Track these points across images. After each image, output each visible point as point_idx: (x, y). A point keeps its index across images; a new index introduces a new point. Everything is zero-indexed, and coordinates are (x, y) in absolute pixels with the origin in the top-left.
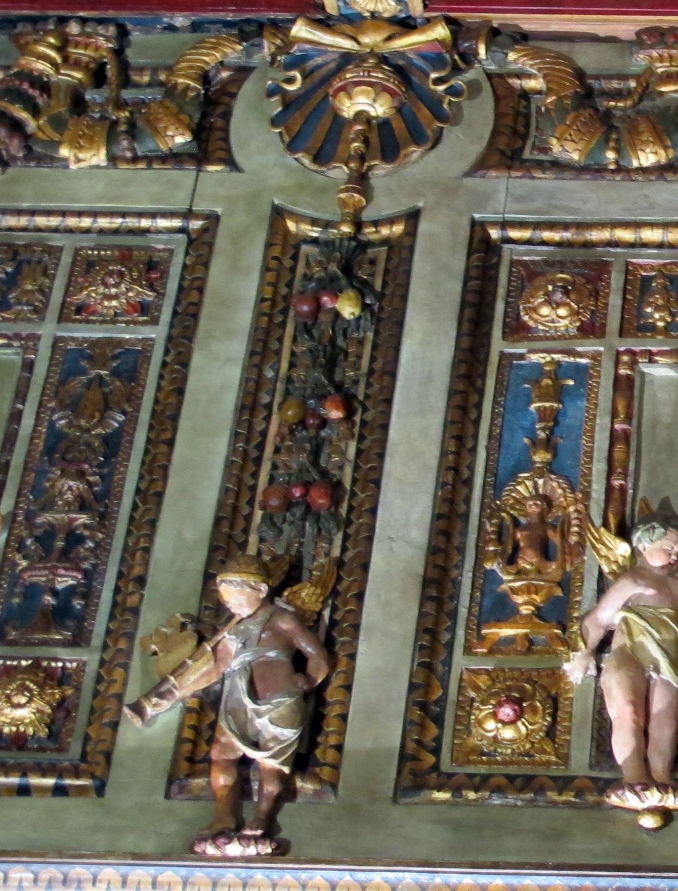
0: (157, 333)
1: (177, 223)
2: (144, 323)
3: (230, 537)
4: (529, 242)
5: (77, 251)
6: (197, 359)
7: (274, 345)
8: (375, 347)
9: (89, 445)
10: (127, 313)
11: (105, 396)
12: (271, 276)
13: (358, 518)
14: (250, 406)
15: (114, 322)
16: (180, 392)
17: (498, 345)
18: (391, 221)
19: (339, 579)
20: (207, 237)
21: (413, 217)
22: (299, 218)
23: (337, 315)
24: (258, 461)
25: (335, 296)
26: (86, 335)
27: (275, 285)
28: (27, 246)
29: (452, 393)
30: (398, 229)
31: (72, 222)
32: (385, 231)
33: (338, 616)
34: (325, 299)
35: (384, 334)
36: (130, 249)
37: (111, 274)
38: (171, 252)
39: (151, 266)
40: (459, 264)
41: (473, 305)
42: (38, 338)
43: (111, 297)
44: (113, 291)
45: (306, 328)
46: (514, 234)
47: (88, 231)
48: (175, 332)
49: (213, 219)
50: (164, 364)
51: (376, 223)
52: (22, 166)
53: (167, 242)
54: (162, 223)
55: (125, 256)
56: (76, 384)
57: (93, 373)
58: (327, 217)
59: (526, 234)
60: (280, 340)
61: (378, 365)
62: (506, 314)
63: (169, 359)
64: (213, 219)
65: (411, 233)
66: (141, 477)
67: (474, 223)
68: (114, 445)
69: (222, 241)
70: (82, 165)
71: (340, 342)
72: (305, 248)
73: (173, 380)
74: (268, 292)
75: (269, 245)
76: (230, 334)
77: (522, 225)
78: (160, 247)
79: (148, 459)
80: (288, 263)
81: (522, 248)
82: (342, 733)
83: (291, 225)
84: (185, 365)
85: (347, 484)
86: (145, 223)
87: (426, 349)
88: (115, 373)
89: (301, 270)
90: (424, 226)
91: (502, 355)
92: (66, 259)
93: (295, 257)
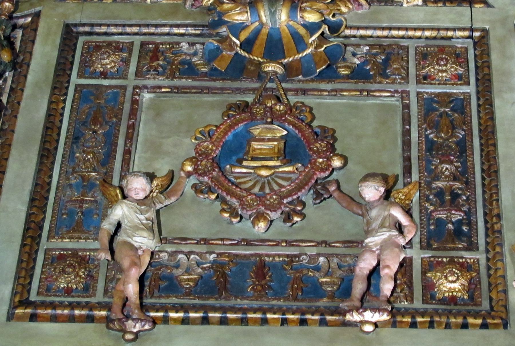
0: (471, 89)
1: (467, 33)
2: (461, 84)
5: (416, 48)
6: (497, 102)
9: (450, 147)
10: (452, 79)
11: (452, 122)
15: (446, 84)
16: (492, 119)
20: (485, 40)
26: (433, 91)
28: (390, 46)
31: (411, 33)
36: (443, 47)
37: (442, 59)
38: (466, 49)
39: (458, 56)
42: (408, 92)
43: (442, 71)
44: (444, 68)
47: (420, 38)
48: (480, 89)
49: (485, 32)
50: (479, 106)
52: (377, 5)
53: (463, 43)
54: (459, 34)
55: (442, 49)
56: (434, 116)
57: (442, 110)
63: (481, 103)
64: (485, 32)
66: (482, 163)
68: (463, 148)
69: (493, 43)
70: (410, 4)
73: (486, 114)
78: (459, 46)
79: (484, 154)
84: (491, 105)
86: (450, 34)
88: (452, 110)
92: (412, 52)
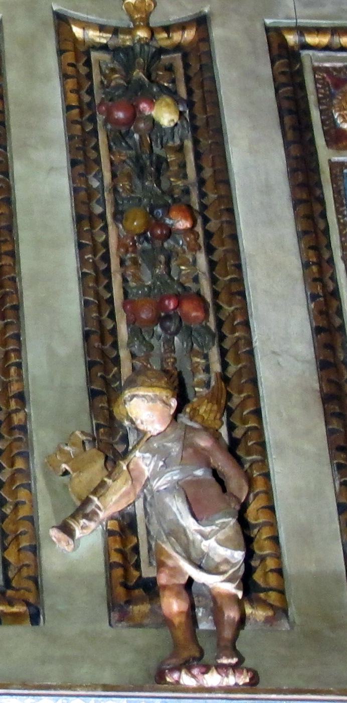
3: (103, 354)
4: (327, 48)
7: (93, 155)
8: (198, 156)
12: (71, 84)
13: (233, 331)
14: (85, 219)
17: (325, 155)
18: (182, 26)
19: (229, 396)
21: (202, 22)
22: (85, 25)
23: (154, 124)
24: (108, 272)
25: (152, 104)
27: (77, 91)
29: (296, 203)
30: (189, 35)
32: (177, 37)
33: (238, 433)
34: (144, 106)
35: (205, 143)
40: (266, 70)
41: (290, 112)
45: (119, 137)
46: (311, 39)
51: (167, 29)
58: (114, 23)
59: (324, 40)
60: (96, 148)
61: (208, 173)
62: (323, 122)
65: (204, 37)
67: (267, 29)
71: (157, 150)
72: (95, 55)
74: (73, 99)
75: (60, 52)
76: (47, 142)
77: (319, 30)
80: (83, 70)
81: (321, 54)
82: (278, 556)
83: (78, 31)
85: (208, 297)
87: (255, 160)
89: (97, 78)
90: (217, 32)
91: (332, 165)
93: (88, 63)
